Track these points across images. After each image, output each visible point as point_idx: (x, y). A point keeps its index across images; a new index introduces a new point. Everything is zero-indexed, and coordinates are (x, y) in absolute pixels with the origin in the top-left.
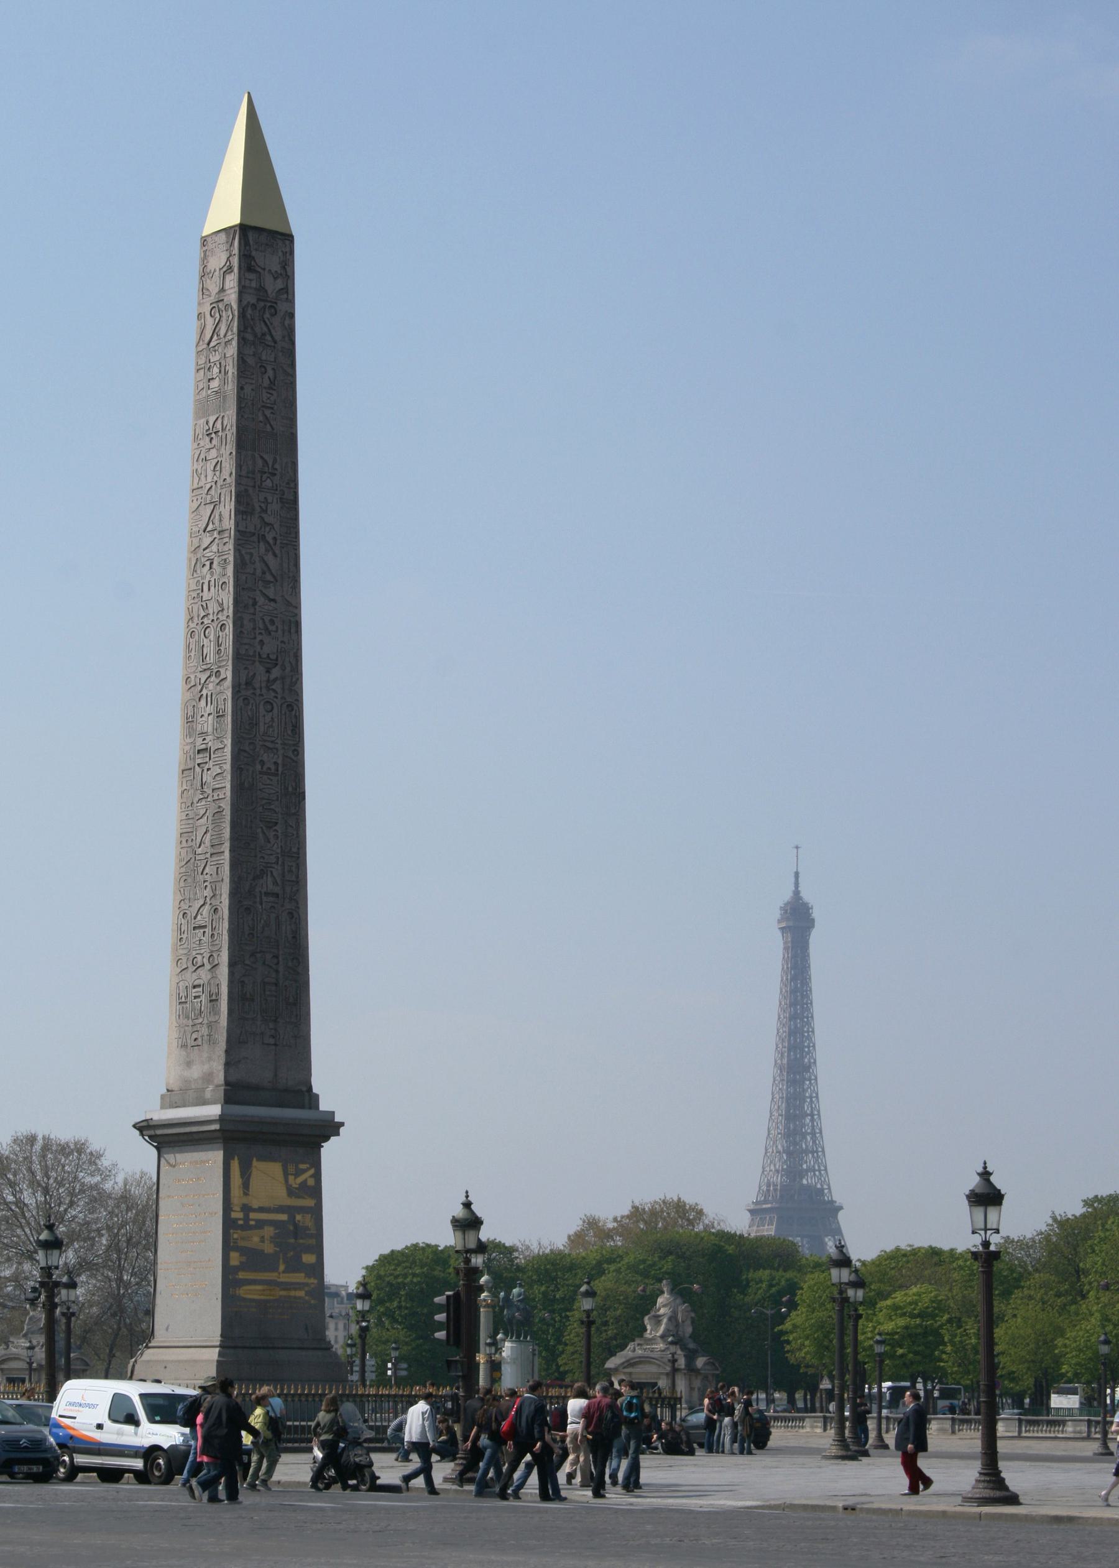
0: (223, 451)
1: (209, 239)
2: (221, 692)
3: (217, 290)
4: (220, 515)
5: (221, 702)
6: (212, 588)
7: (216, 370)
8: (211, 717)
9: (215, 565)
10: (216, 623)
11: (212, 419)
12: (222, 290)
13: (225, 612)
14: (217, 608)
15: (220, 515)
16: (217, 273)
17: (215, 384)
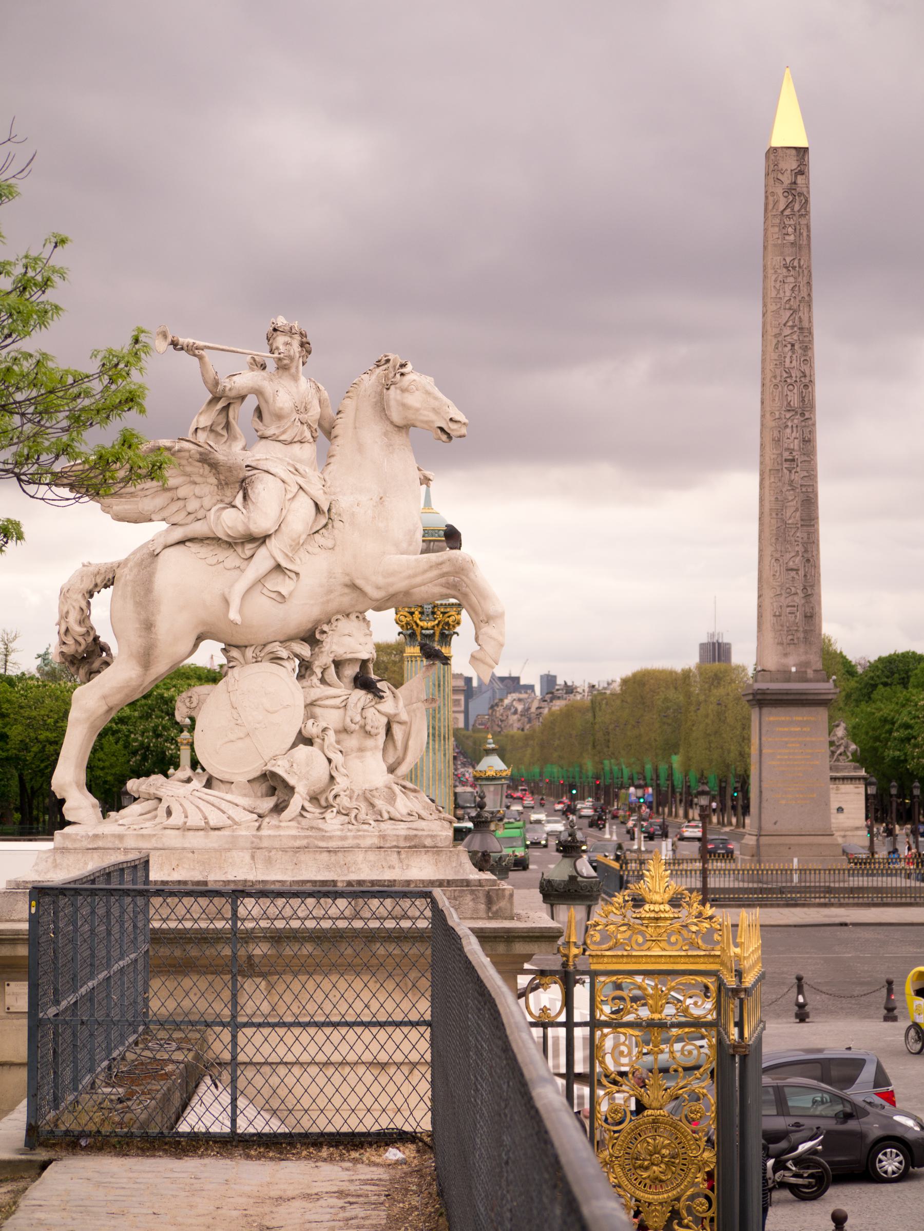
0: (800, 279)
1: (780, 150)
2: (805, 426)
3: (789, 182)
4: (800, 318)
5: (807, 430)
6: (794, 362)
7: (790, 230)
8: (796, 441)
9: (796, 347)
10: (799, 384)
11: (788, 259)
12: (795, 183)
13: (808, 379)
14: (799, 374)
15: (800, 318)
16: (789, 172)
17: (792, 238)
